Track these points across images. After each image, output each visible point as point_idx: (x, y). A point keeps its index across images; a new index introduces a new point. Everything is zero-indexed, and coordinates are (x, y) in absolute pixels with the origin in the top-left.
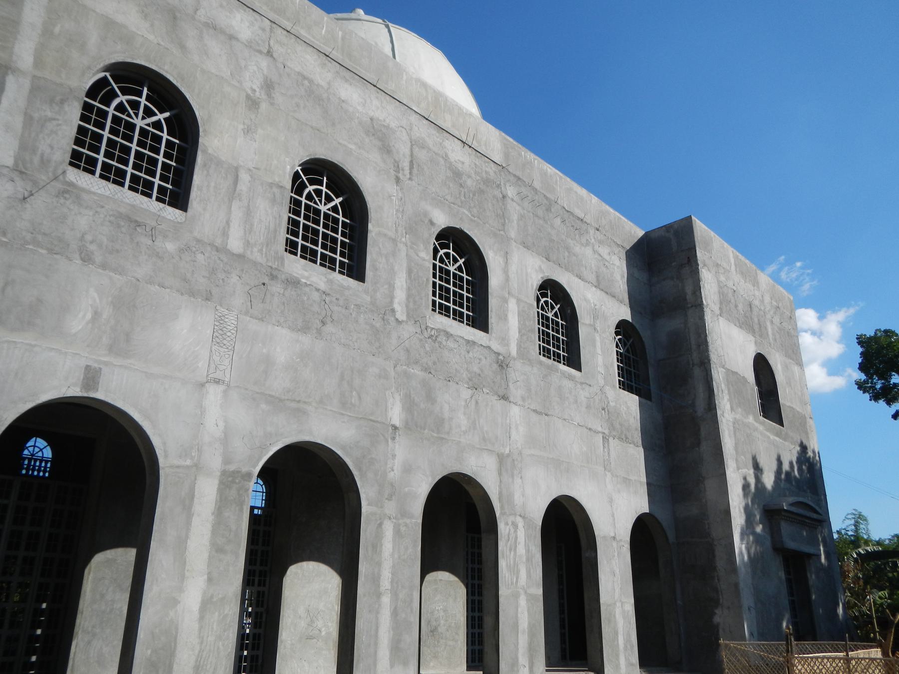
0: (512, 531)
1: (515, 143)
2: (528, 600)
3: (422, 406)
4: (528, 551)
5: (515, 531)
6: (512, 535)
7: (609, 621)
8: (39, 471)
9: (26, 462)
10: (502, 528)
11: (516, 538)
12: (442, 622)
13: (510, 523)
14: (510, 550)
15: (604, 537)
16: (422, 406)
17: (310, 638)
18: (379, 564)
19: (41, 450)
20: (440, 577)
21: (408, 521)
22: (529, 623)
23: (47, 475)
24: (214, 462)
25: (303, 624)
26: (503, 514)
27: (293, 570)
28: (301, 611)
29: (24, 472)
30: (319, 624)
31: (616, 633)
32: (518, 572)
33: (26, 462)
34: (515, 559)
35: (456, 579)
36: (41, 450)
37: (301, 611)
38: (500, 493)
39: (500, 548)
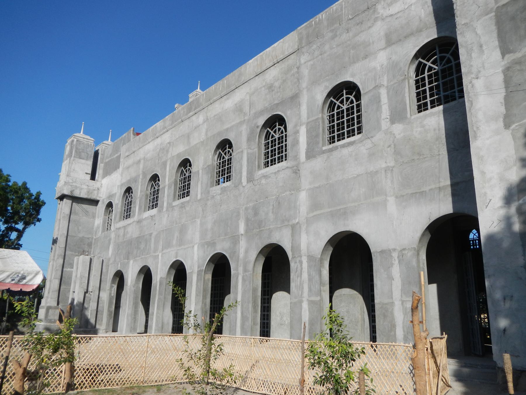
0: (299, 266)
1: (308, 22)
2: (309, 304)
3: (253, 219)
4: (309, 275)
5: (301, 265)
6: (299, 268)
7: (385, 316)
8: (473, 246)
9: (471, 242)
10: (293, 265)
11: (302, 269)
12: (346, 318)
13: (298, 261)
14: (298, 277)
15: (377, 252)
16: (253, 219)
17: (281, 325)
18: (237, 294)
19: (475, 234)
20: (343, 293)
21: (247, 273)
22: (309, 318)
23: (478, 247)
24: (196, 269)
25: (279, 318)
26: (293, 258)
27: (274, 296)
28: (278, 313)
29: (472, 247)
30: (285, 319)
31: (393, 326)
32: (303, 288)
33: (471, 242)
34: (301, 281)
35: (355, 292)
36: (475, 234)
37: (278, 313)
38: (292, 247)
39: (291, 277)
